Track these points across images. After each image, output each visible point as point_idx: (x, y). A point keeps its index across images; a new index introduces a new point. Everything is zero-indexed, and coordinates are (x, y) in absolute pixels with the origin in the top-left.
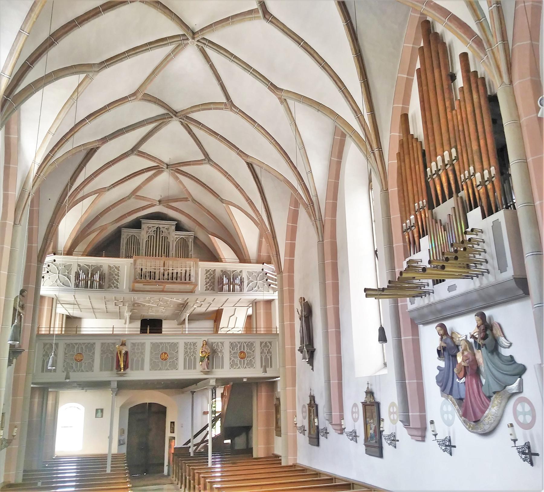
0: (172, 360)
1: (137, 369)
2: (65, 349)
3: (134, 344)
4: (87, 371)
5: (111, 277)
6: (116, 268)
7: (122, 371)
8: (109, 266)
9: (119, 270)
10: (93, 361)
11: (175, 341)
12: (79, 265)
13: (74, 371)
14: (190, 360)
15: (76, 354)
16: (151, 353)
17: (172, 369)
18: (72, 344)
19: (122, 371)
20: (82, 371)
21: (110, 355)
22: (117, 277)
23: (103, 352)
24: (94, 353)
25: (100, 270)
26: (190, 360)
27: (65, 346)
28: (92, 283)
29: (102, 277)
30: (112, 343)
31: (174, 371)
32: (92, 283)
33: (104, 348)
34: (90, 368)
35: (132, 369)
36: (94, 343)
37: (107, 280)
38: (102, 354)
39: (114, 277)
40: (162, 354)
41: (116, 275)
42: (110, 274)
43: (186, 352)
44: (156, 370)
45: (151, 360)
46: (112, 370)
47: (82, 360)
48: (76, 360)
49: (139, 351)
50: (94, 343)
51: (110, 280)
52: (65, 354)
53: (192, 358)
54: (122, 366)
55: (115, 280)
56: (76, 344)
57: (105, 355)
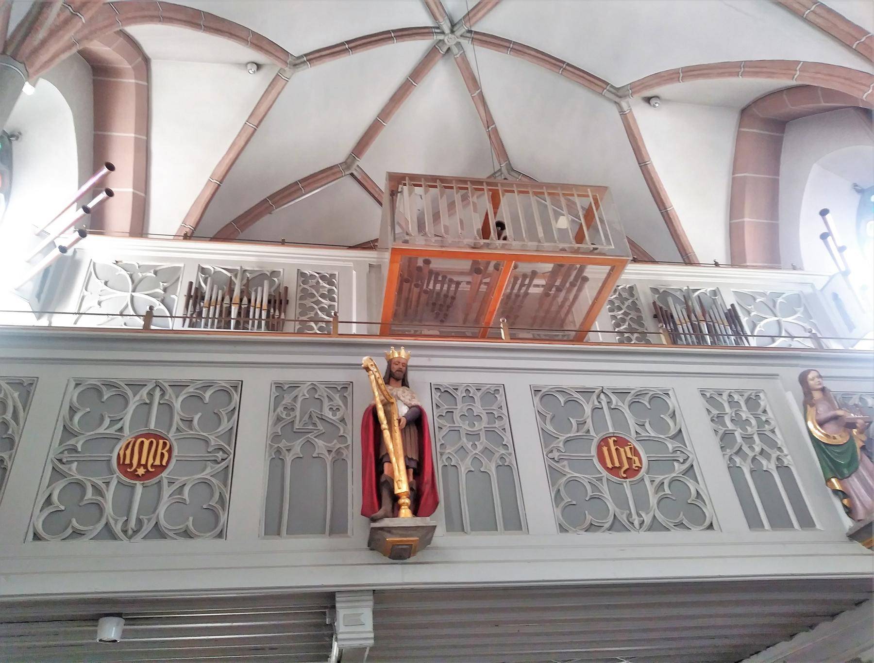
0: (667, 478)
1: (486, 523)
2: (73, 411)
3: (445, 392)
4: (187, 534)
5: (308, 302)
6: (323, 277)
7: (405, 512)
8: (301, 274)
9: (331, 283)
10: (226, 475)
11: (655, 383)
12: (203, 270)
13: (109, 533)
14: (761, 476)
15: (128, 435)
16: (546, 437)
17: (680, 525)
18: (110, 385)
19: (405, 512)
20: (158, 533)
21: (321, 444)
22: (325, 303)
23: (284, 430)
24: (232, 435)
25: (272, 283)
26: (761, 476)
27: (74, 394)
28: (244, 314)
29: (278, 301)
30: (332, 387)
31: (697, 534)
32: (244, 314)
33: (290, 409)
34: (212, 520)
35: (455, 525)
36: (238, 386)
37: (292, 311)
38: (276, 438)
39: (317, 303)
40: (604, 441)
41: (323, 296)
42: (305, 294)
43: (726, 439)
44: (591, 528)
45: (554, 474)
46: (338, 528)
47: (162, 468)
48: (123, 466)
49: (481, 426)
50: (238, 386)
51: (304, 310)
52: (68, 432)
53: (770, 466)
54: (402, 486)
55: (322, 309)
56: (136, 386)
57: (297, 446)
